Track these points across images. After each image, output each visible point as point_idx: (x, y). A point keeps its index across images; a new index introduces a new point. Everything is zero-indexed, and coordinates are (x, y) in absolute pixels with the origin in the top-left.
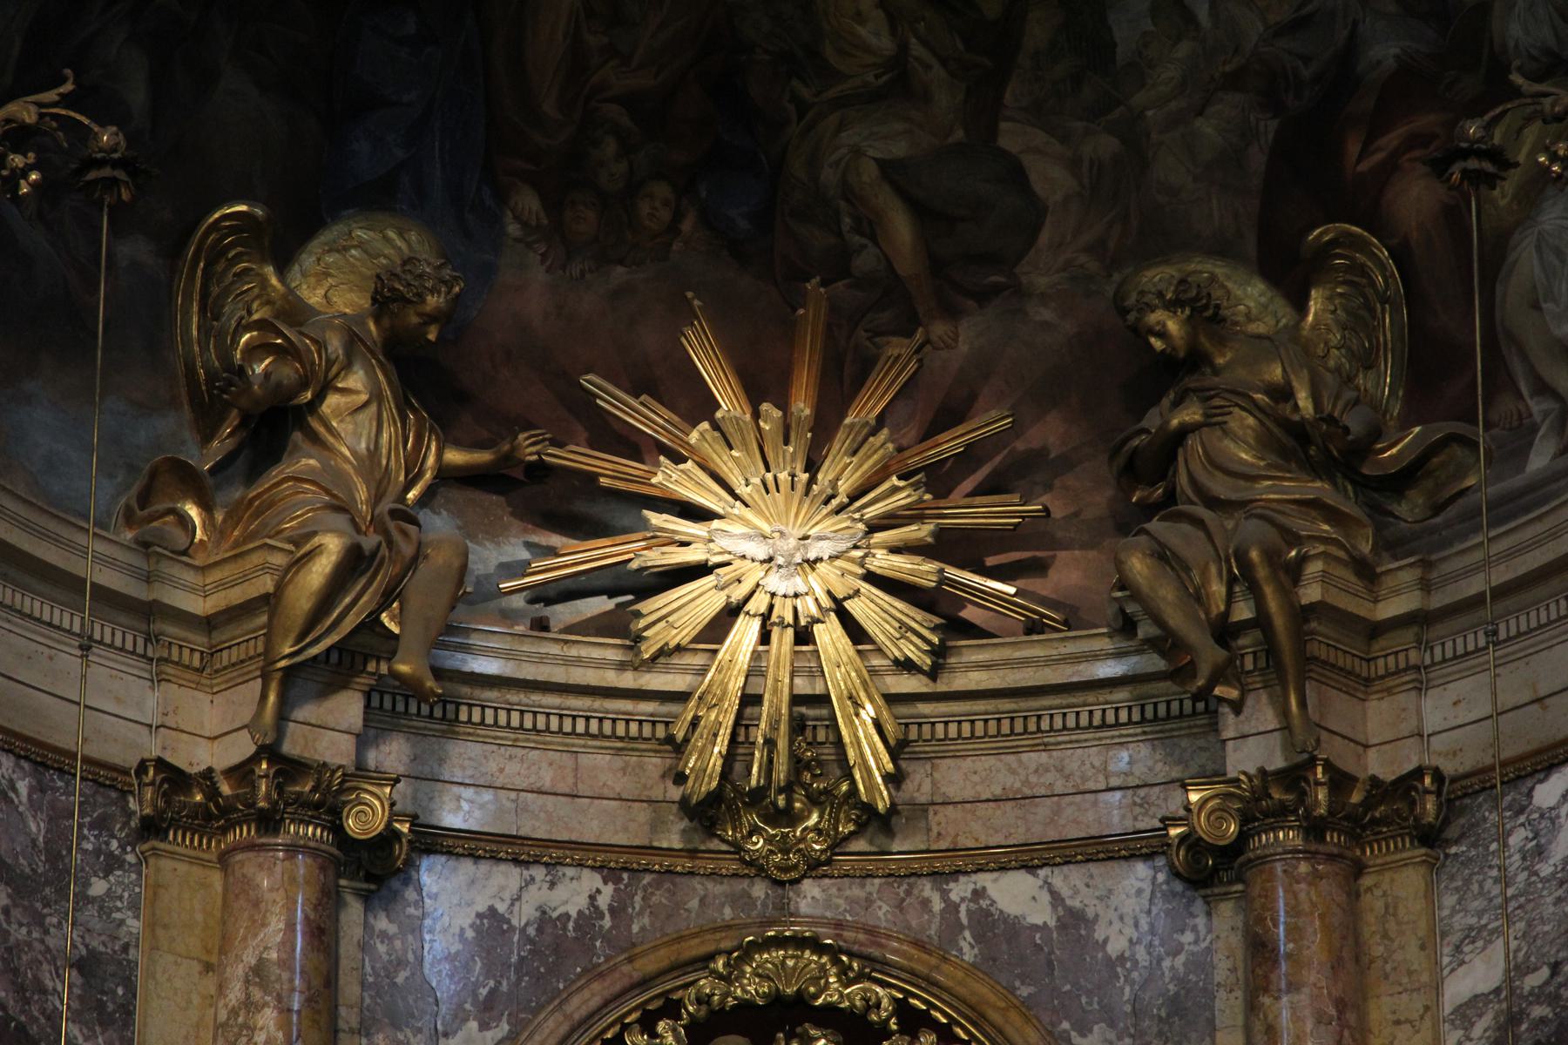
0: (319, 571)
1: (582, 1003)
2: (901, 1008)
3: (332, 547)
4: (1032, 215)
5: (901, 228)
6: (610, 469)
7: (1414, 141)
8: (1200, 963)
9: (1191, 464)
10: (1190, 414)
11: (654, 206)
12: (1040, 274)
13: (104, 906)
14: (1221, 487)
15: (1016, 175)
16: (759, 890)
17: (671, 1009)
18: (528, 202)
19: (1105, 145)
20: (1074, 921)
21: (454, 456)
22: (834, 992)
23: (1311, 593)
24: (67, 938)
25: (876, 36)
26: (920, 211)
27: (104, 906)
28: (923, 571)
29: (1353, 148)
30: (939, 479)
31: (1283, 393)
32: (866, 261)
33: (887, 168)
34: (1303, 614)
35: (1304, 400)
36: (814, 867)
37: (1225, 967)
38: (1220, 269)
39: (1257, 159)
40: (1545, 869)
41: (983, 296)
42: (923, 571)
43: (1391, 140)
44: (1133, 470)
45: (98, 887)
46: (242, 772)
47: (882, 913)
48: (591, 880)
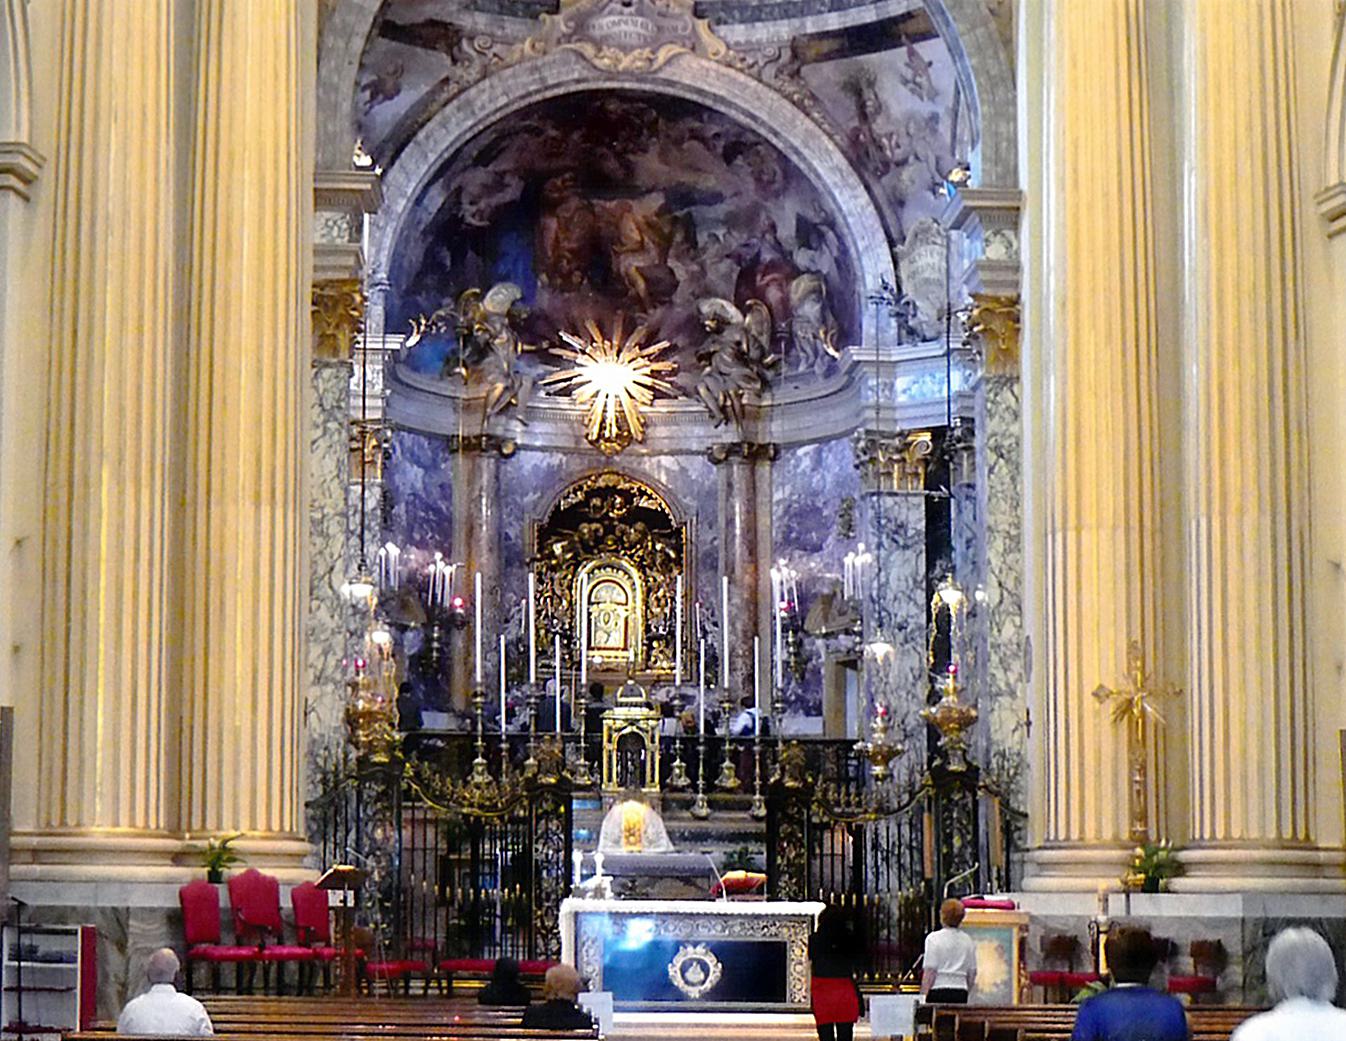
0: (497, 392)
1: (558, 488)
2: (639, 489)
3: (500, 386)
4: (676, 285)
5: (641, 284)
6: (566, 354)
7: (774, 280)
8: (715, 483)
9: (715, 360)
10: (717, 347)
11: (576, 277)
12: (677, 298)
13: (444, 471)
14: (724, 369)
15: (671, 272)
16: (603, 458)
17: (581, 488)
18: (544, 277)
19: (695, 268)
20: (683, 470)
21: (526, 347)
22: (623, 485)
23: (744, 401)
24: (437, 479)
25: (636, 236)
26: (646, 280)
27: (444, 471)
28: (649, 381)
29: (759, 278)
30: (650, 358)
31: (739, 344)
32: (632, 292)
33: (637, 268)
34: (742, 406)
35: (744, 346)
36: (617, 453)
37: (721, 486)
38: (724, 303)
39: (735, 276)
40: (799, 470)
41: (663, 303)
42: (649, 381)
43: (768, 278)
44: (700, 359)
45: (443, 466)
46: (478, 437)
47: (635, 465)
48: (560, 456)
